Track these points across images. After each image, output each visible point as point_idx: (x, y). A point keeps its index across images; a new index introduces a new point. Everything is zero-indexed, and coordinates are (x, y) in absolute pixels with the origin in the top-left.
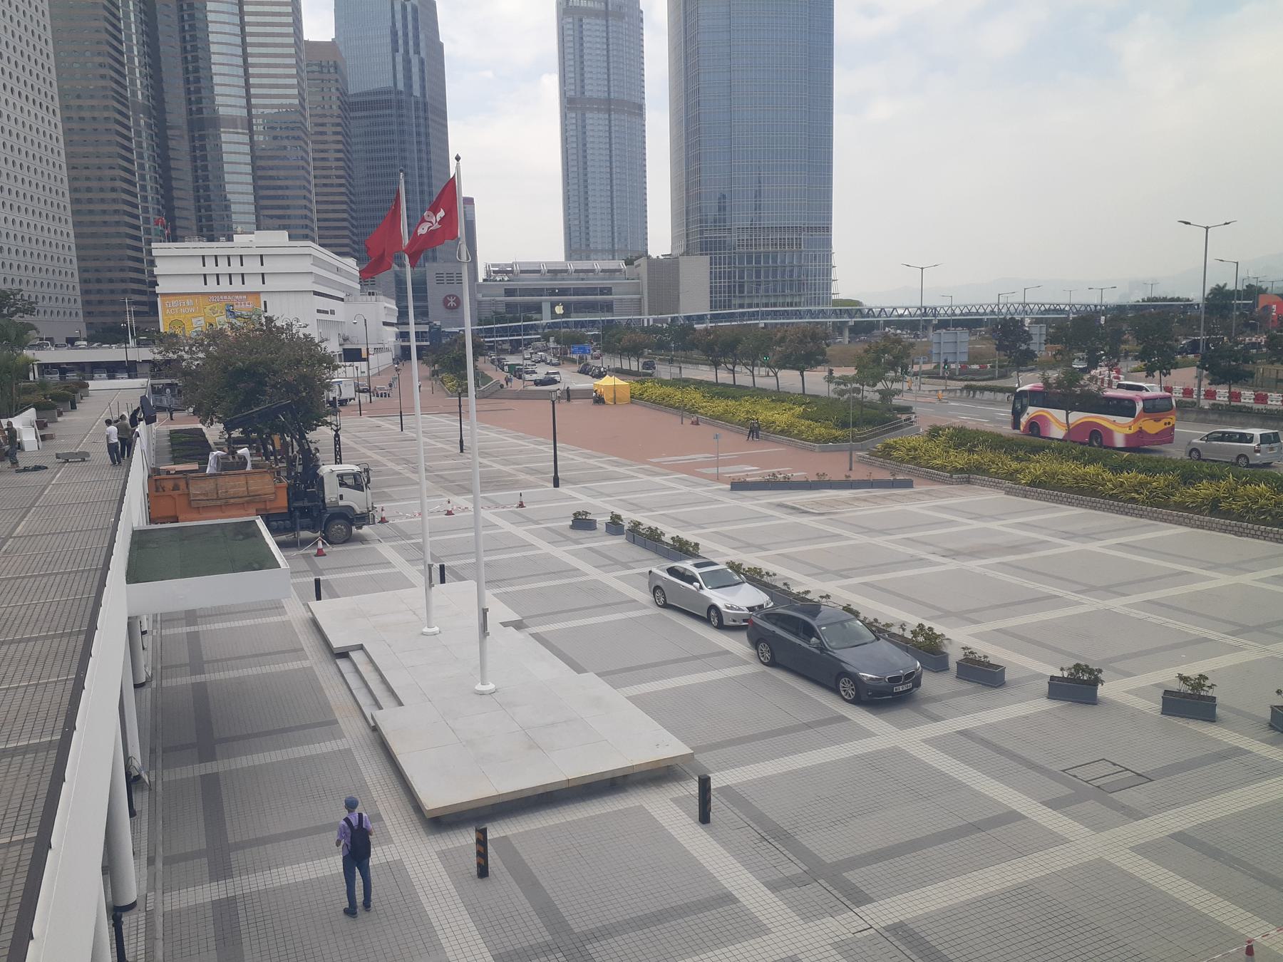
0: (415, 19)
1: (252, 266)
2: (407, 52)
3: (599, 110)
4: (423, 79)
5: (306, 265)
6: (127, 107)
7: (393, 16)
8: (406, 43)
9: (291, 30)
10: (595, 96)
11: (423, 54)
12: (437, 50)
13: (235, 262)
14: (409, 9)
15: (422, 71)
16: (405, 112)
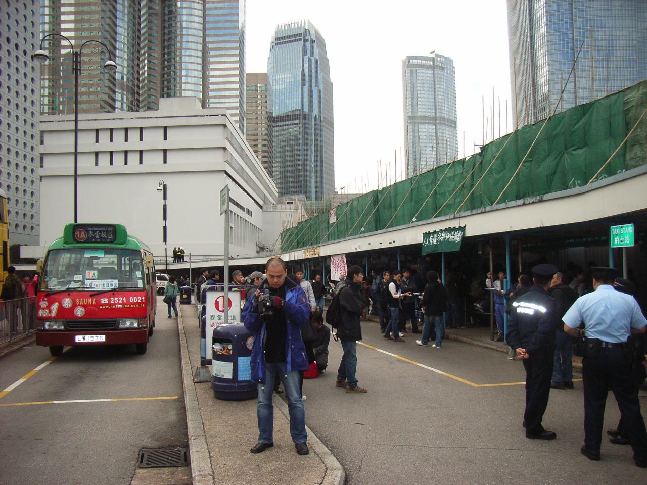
0: (317, 67)
1: (153, 139)
2: (310, 86)
3: (429, 123)
4: (320, 102)
5: (216, 137)
6: (115, 85)
7: (303, 66)
8: (310, 81)
9: (237, 59)
10: (427, 114)
11: (321, 87)
12: (329, 86)
13: (134, 136)
14: (313, 61)
15: (320, 97)
16: (307, 121)
